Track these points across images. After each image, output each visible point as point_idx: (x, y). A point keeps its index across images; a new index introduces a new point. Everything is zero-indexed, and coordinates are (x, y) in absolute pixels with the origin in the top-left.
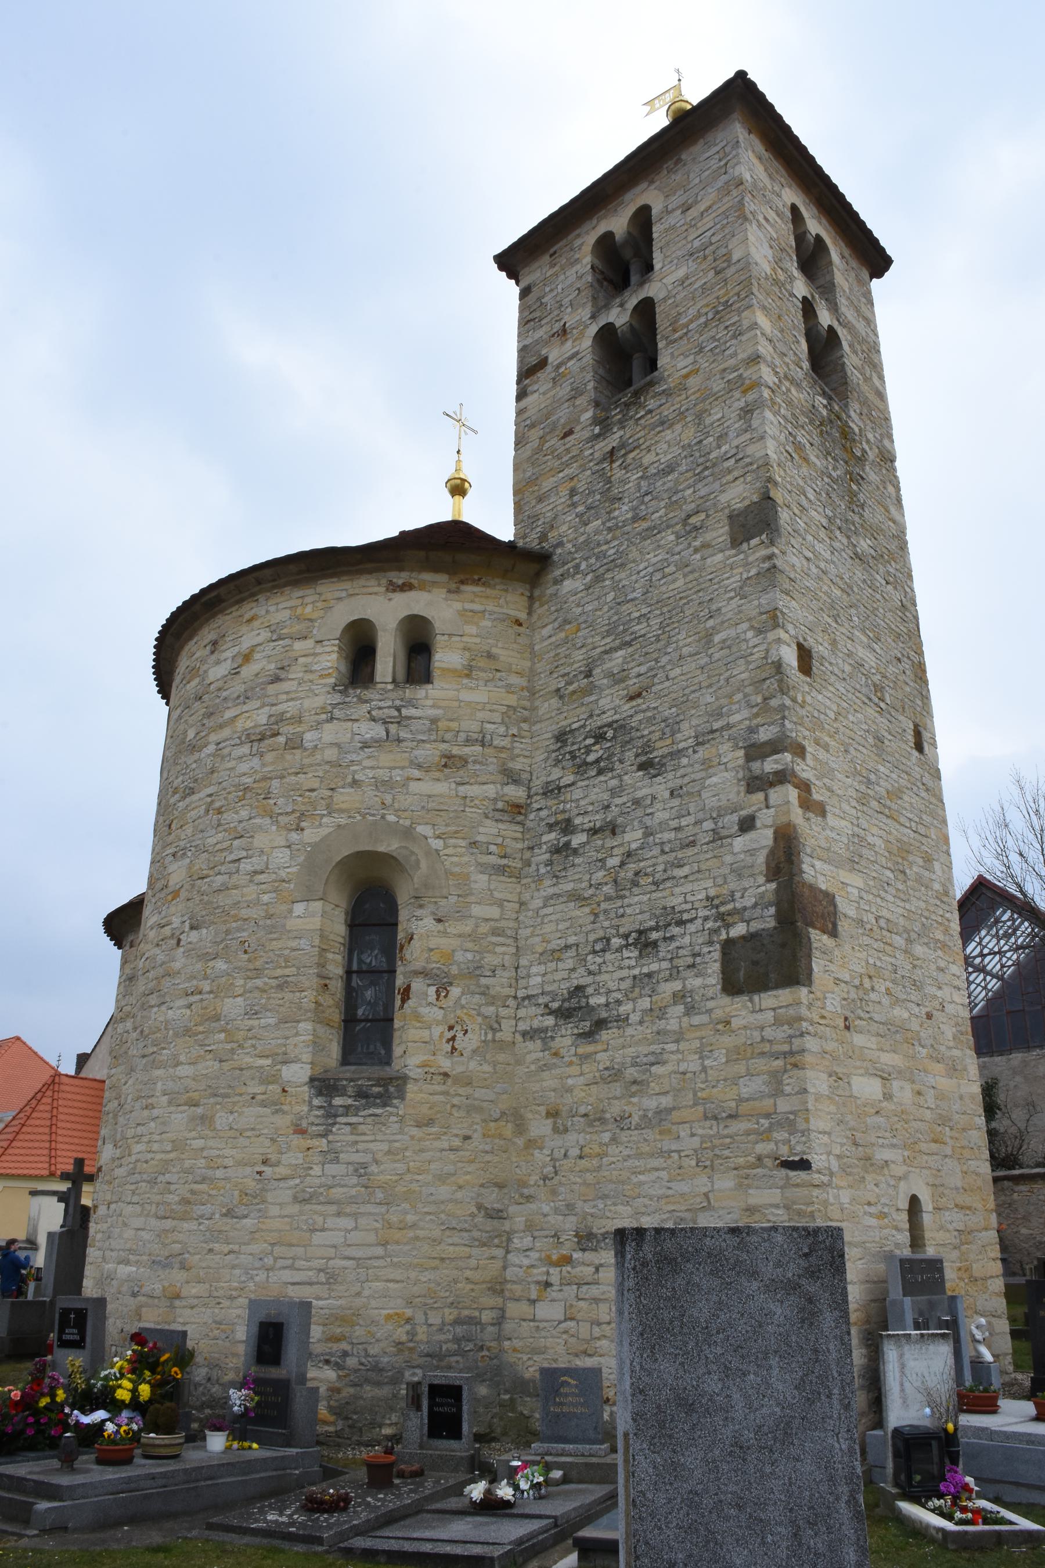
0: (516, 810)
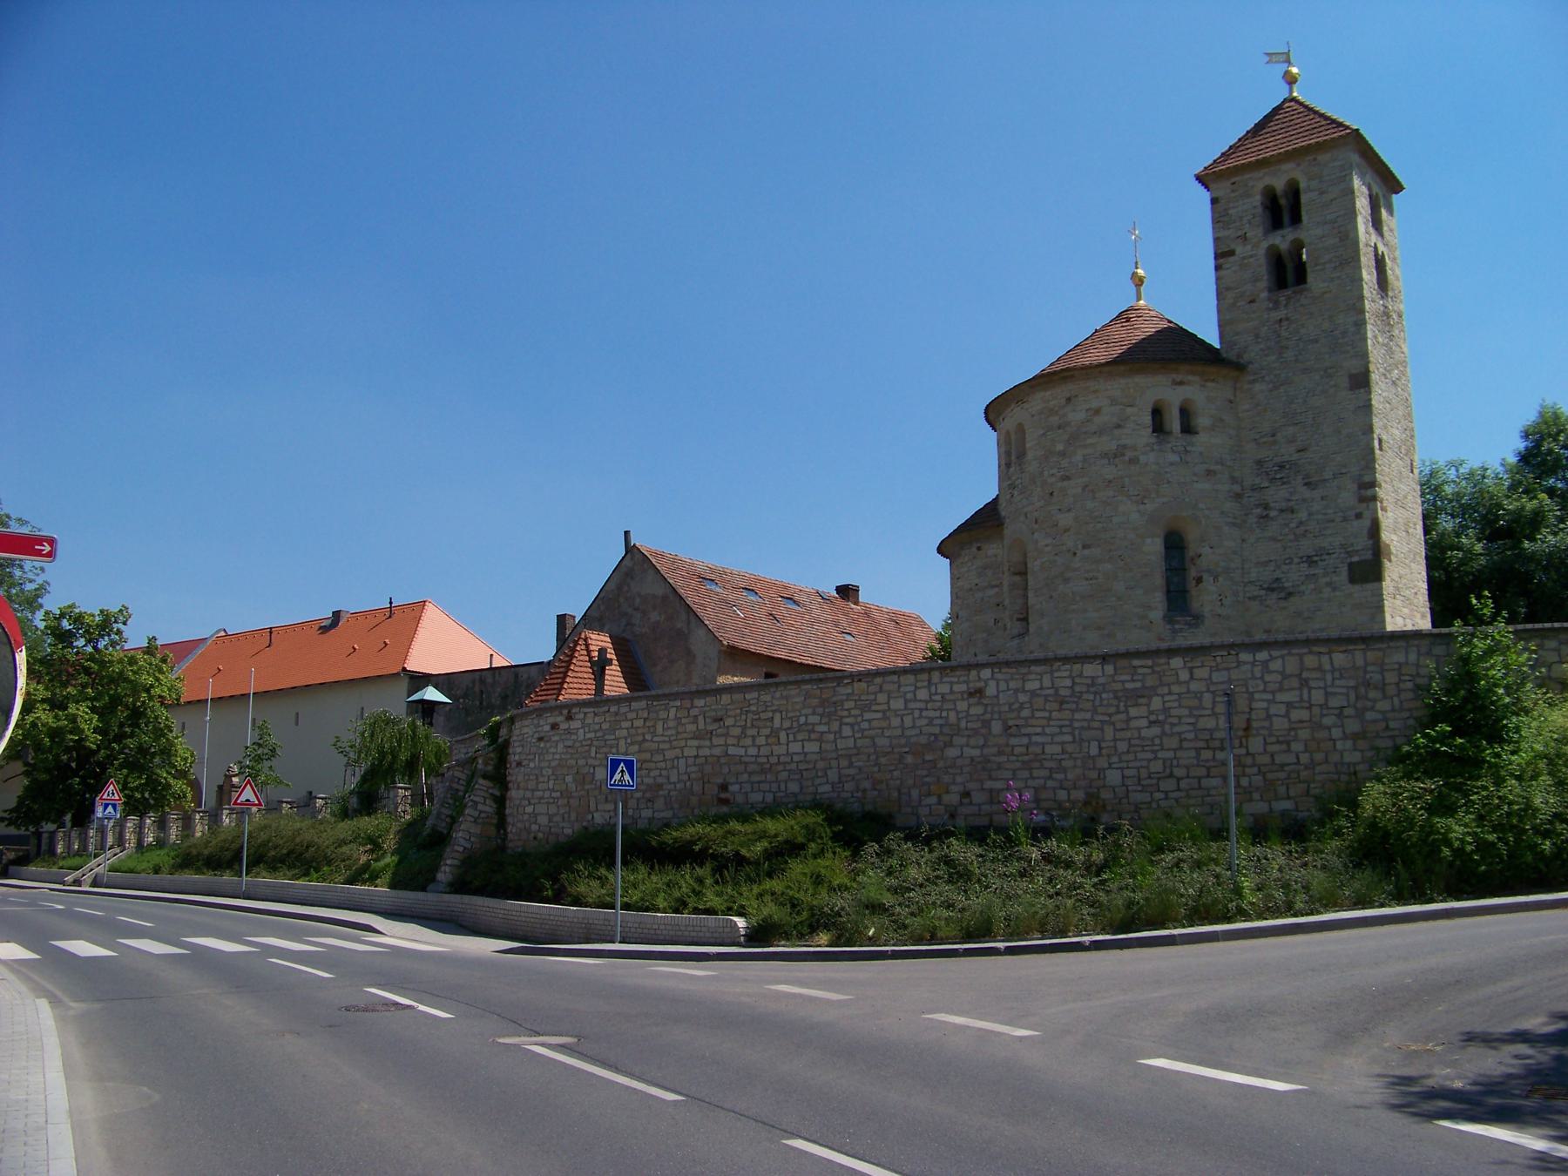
0: (1238, 496)
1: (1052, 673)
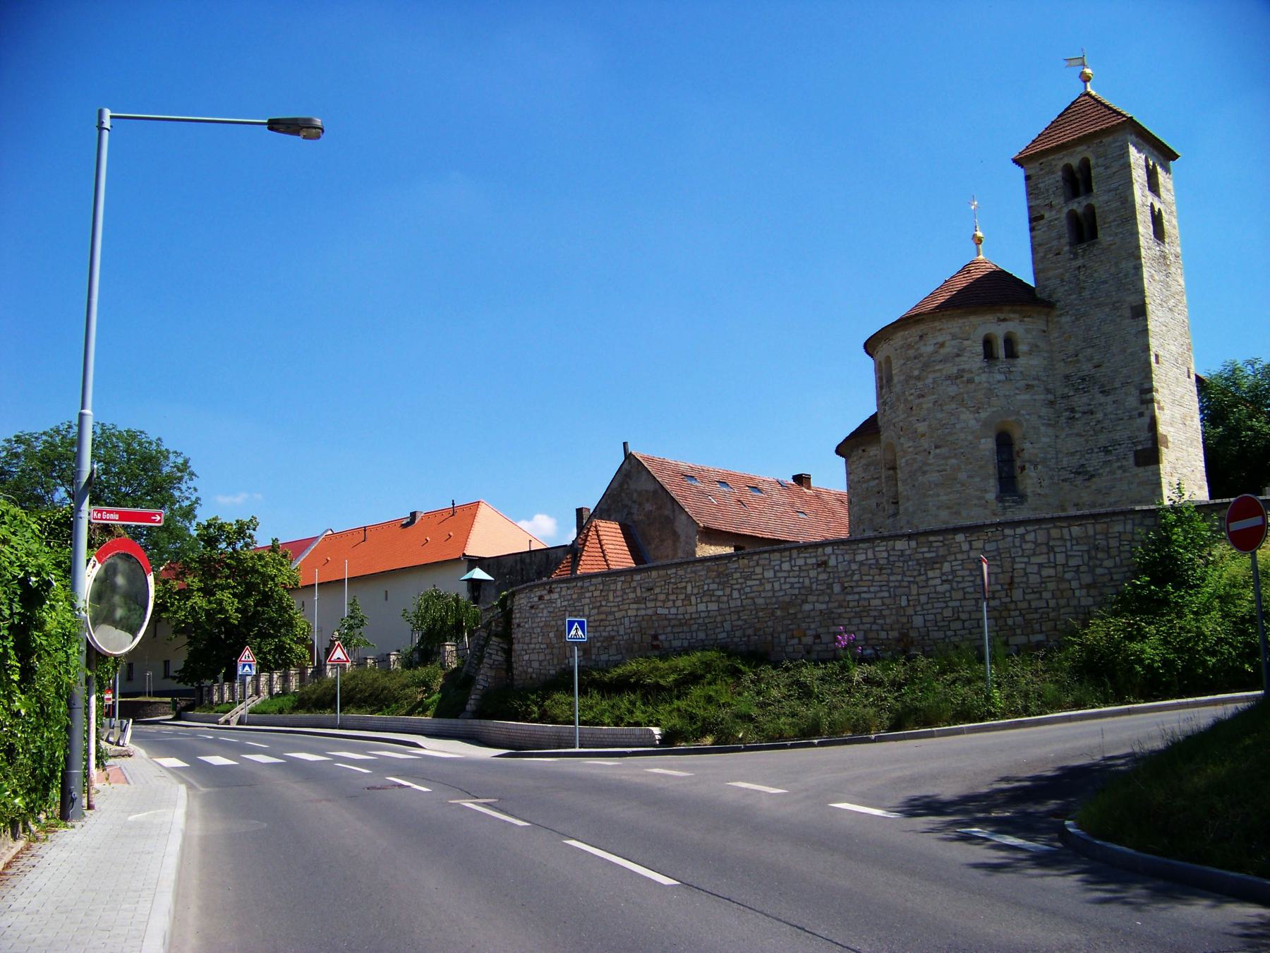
0: (1052, 403)
1: (873, 548)
